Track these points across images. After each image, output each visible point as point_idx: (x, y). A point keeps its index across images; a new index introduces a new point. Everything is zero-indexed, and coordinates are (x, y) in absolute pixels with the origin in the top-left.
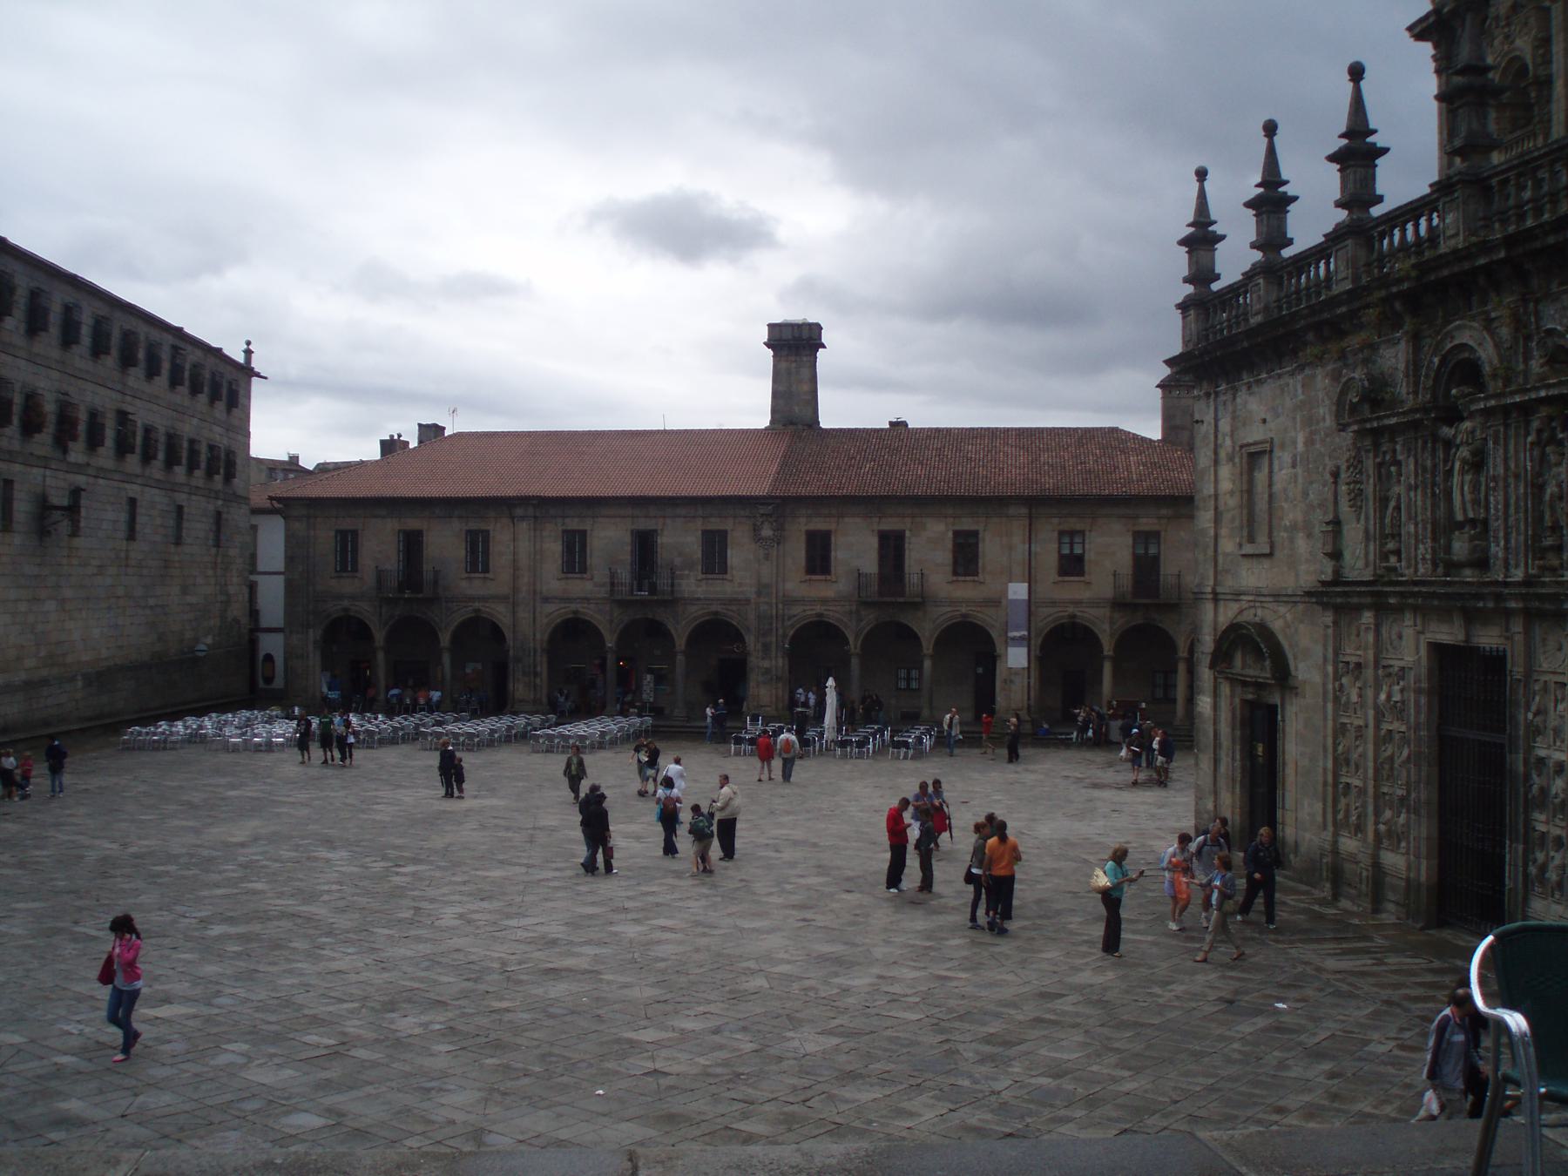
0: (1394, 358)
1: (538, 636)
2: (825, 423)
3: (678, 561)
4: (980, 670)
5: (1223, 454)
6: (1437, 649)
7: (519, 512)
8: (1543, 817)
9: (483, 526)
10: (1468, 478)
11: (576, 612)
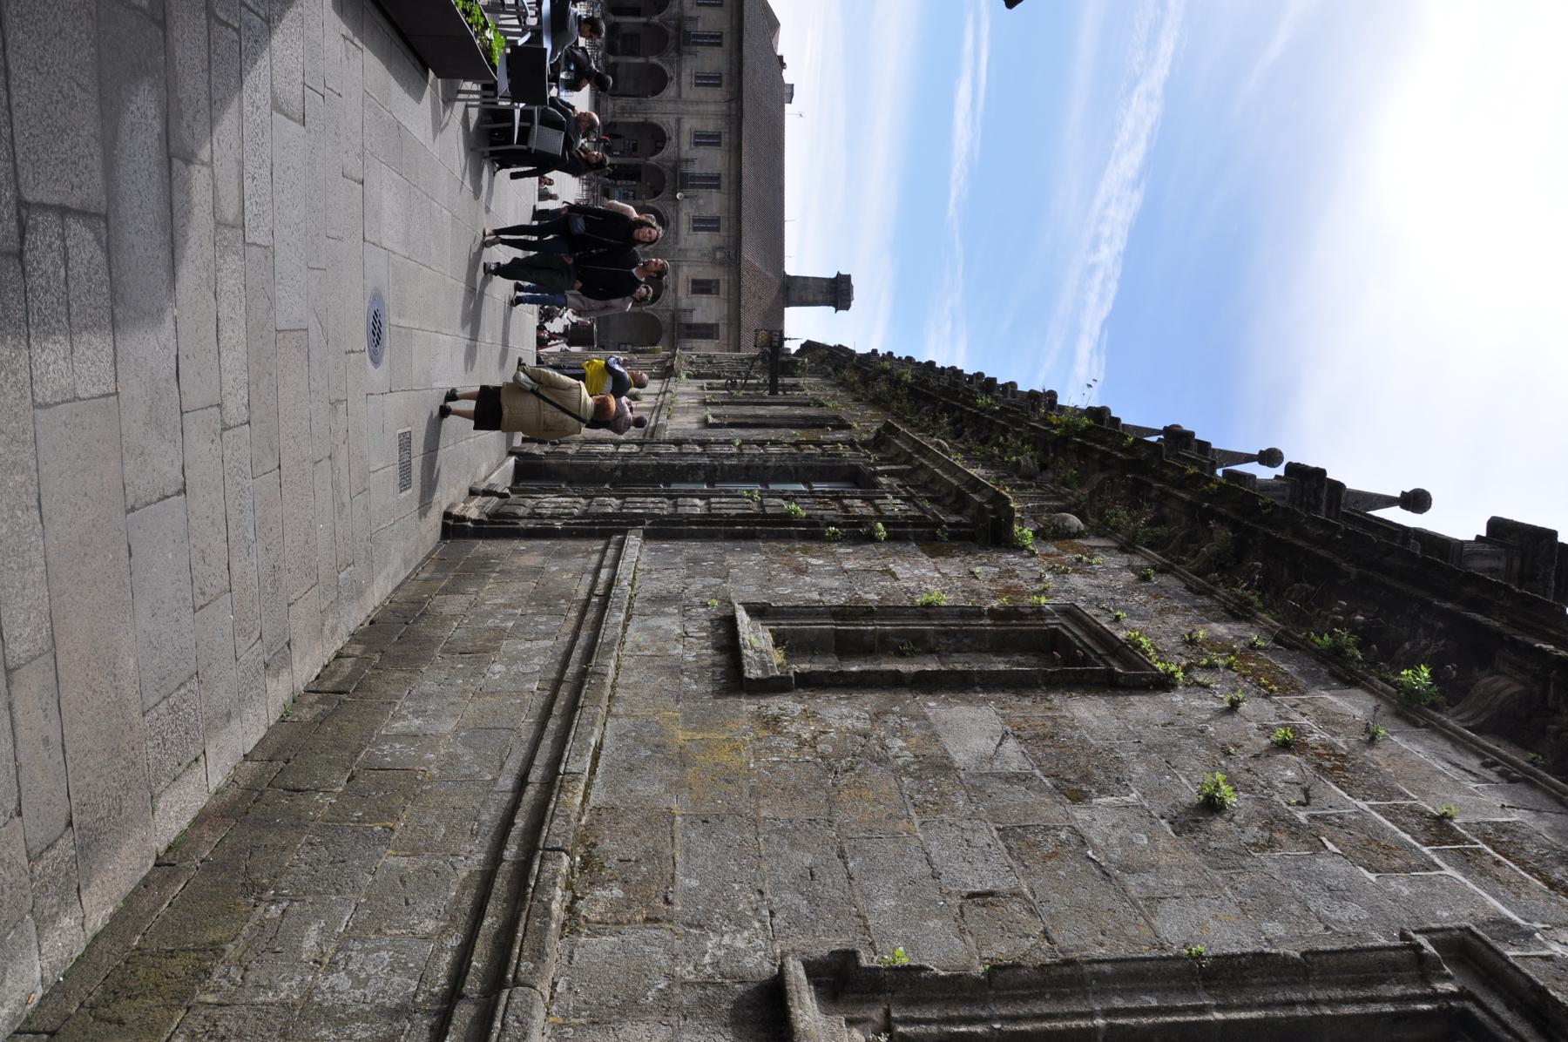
1: (655, 116)
2: (786, 309)
3: (701, 202)
7: (733, 105)
9: (724, 84)
11: (670, 139)
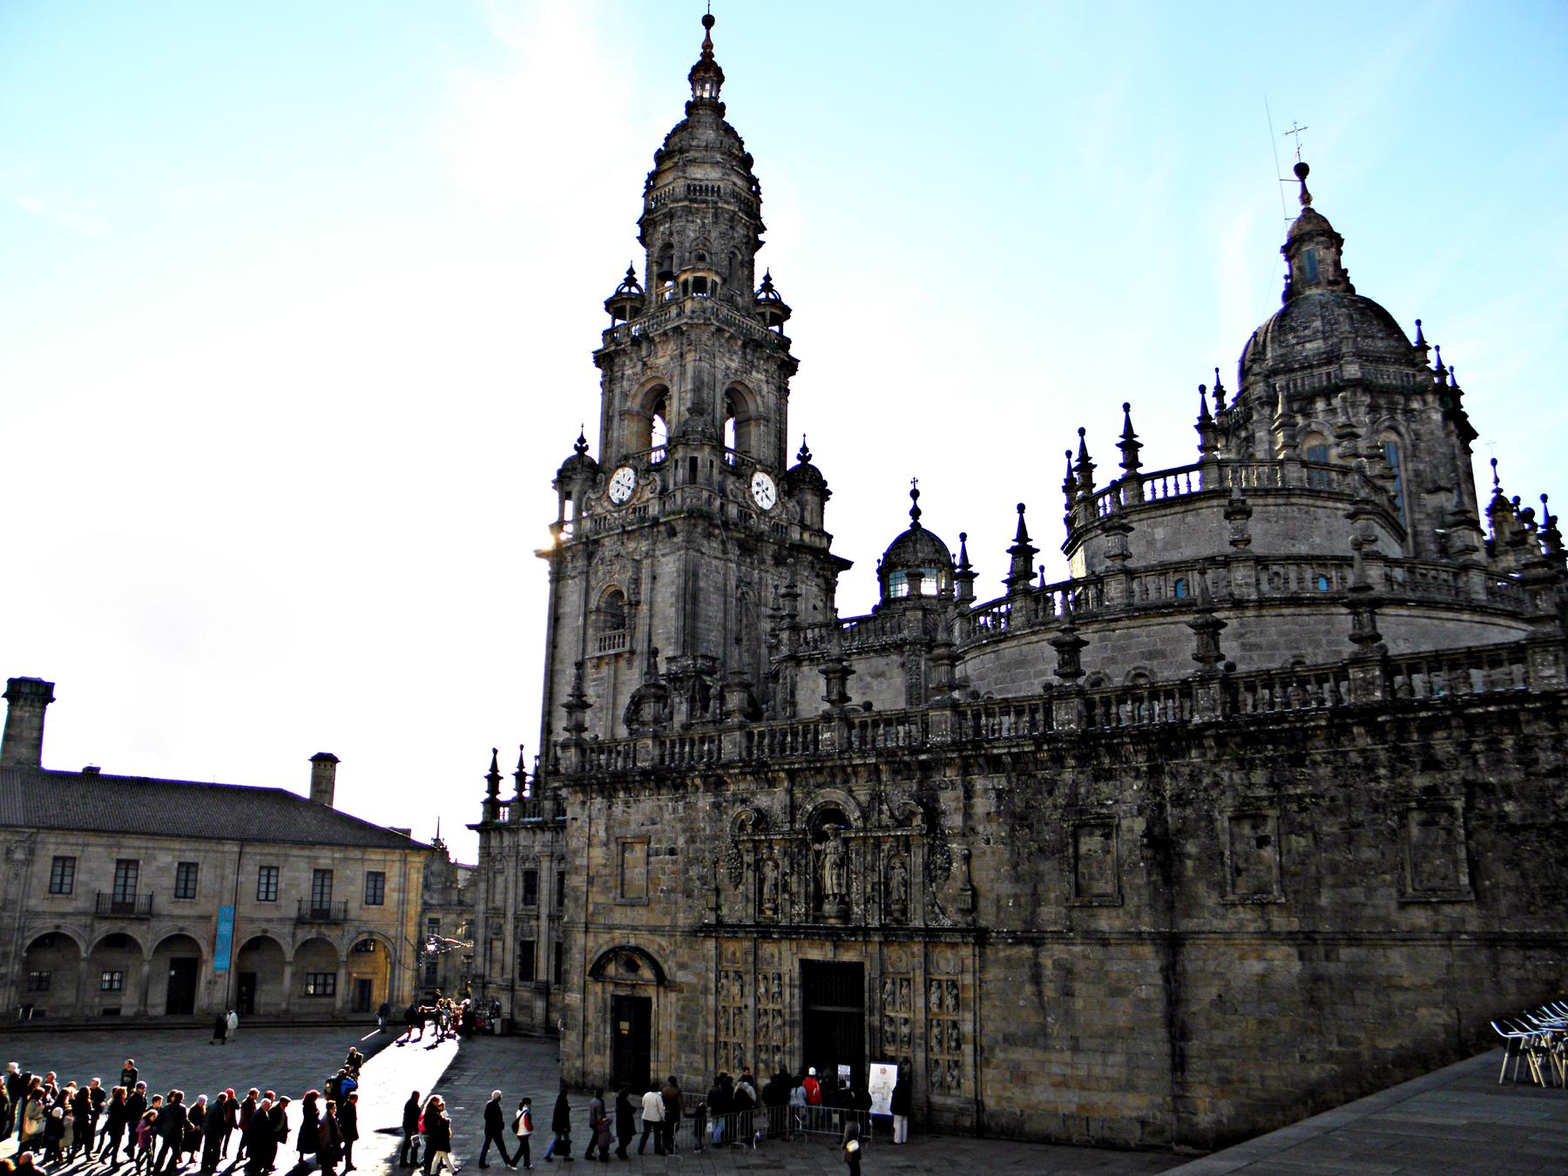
0: (773, 800)
4: (173, 973)
5: (595, 841)
6: (806, 964)
8: (893, 1048)
10: (835, 872)
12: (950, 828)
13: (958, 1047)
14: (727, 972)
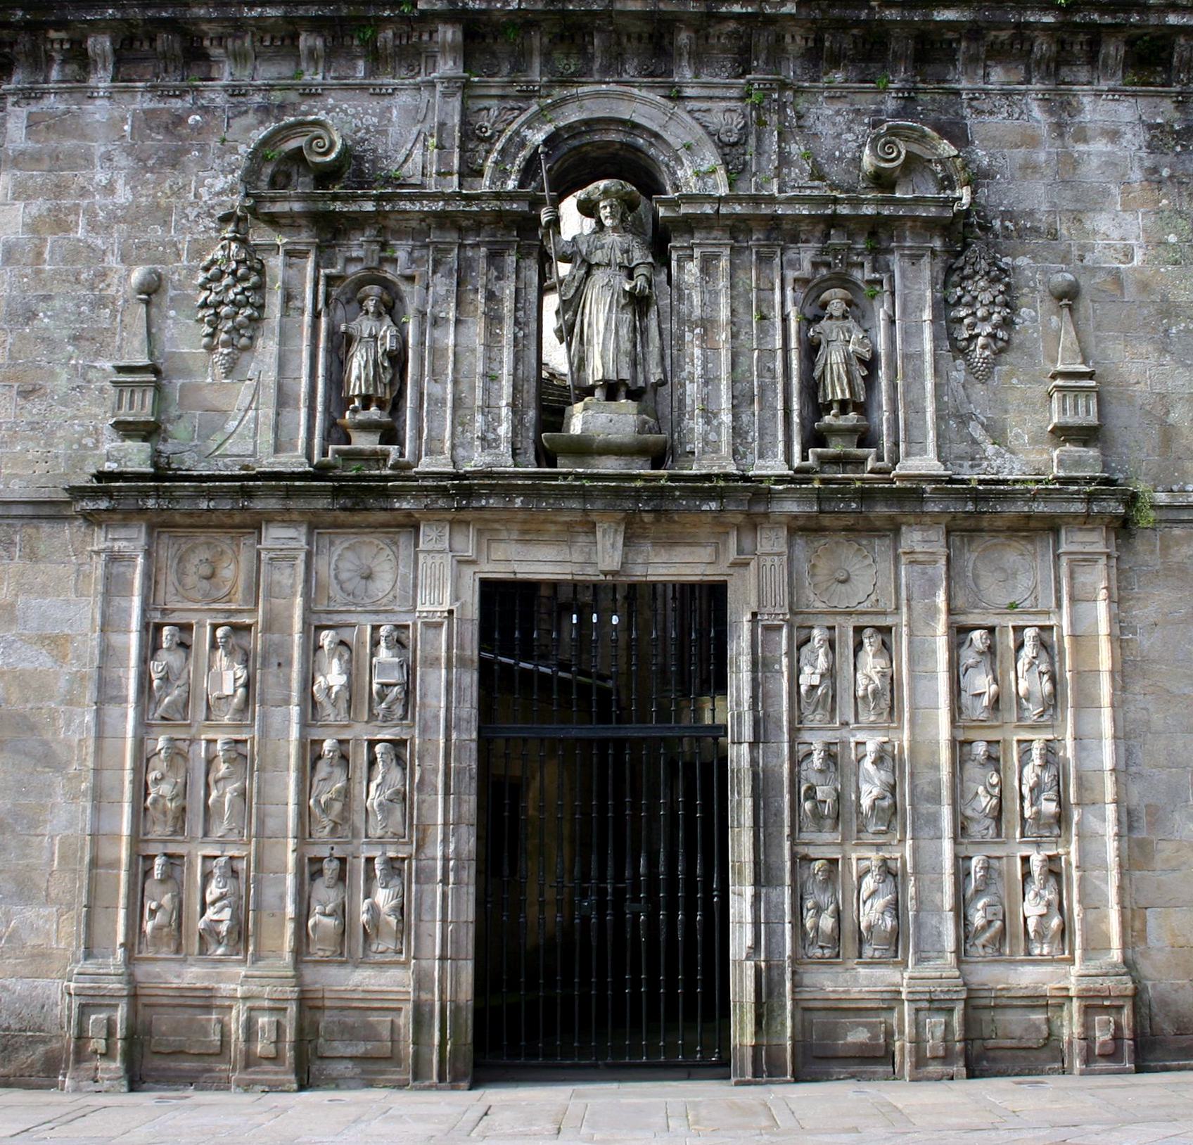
8: (827, 836)
10: (627, 316)
12: (1007, 215)
13: (1061, 819)
14: (186, 628)
